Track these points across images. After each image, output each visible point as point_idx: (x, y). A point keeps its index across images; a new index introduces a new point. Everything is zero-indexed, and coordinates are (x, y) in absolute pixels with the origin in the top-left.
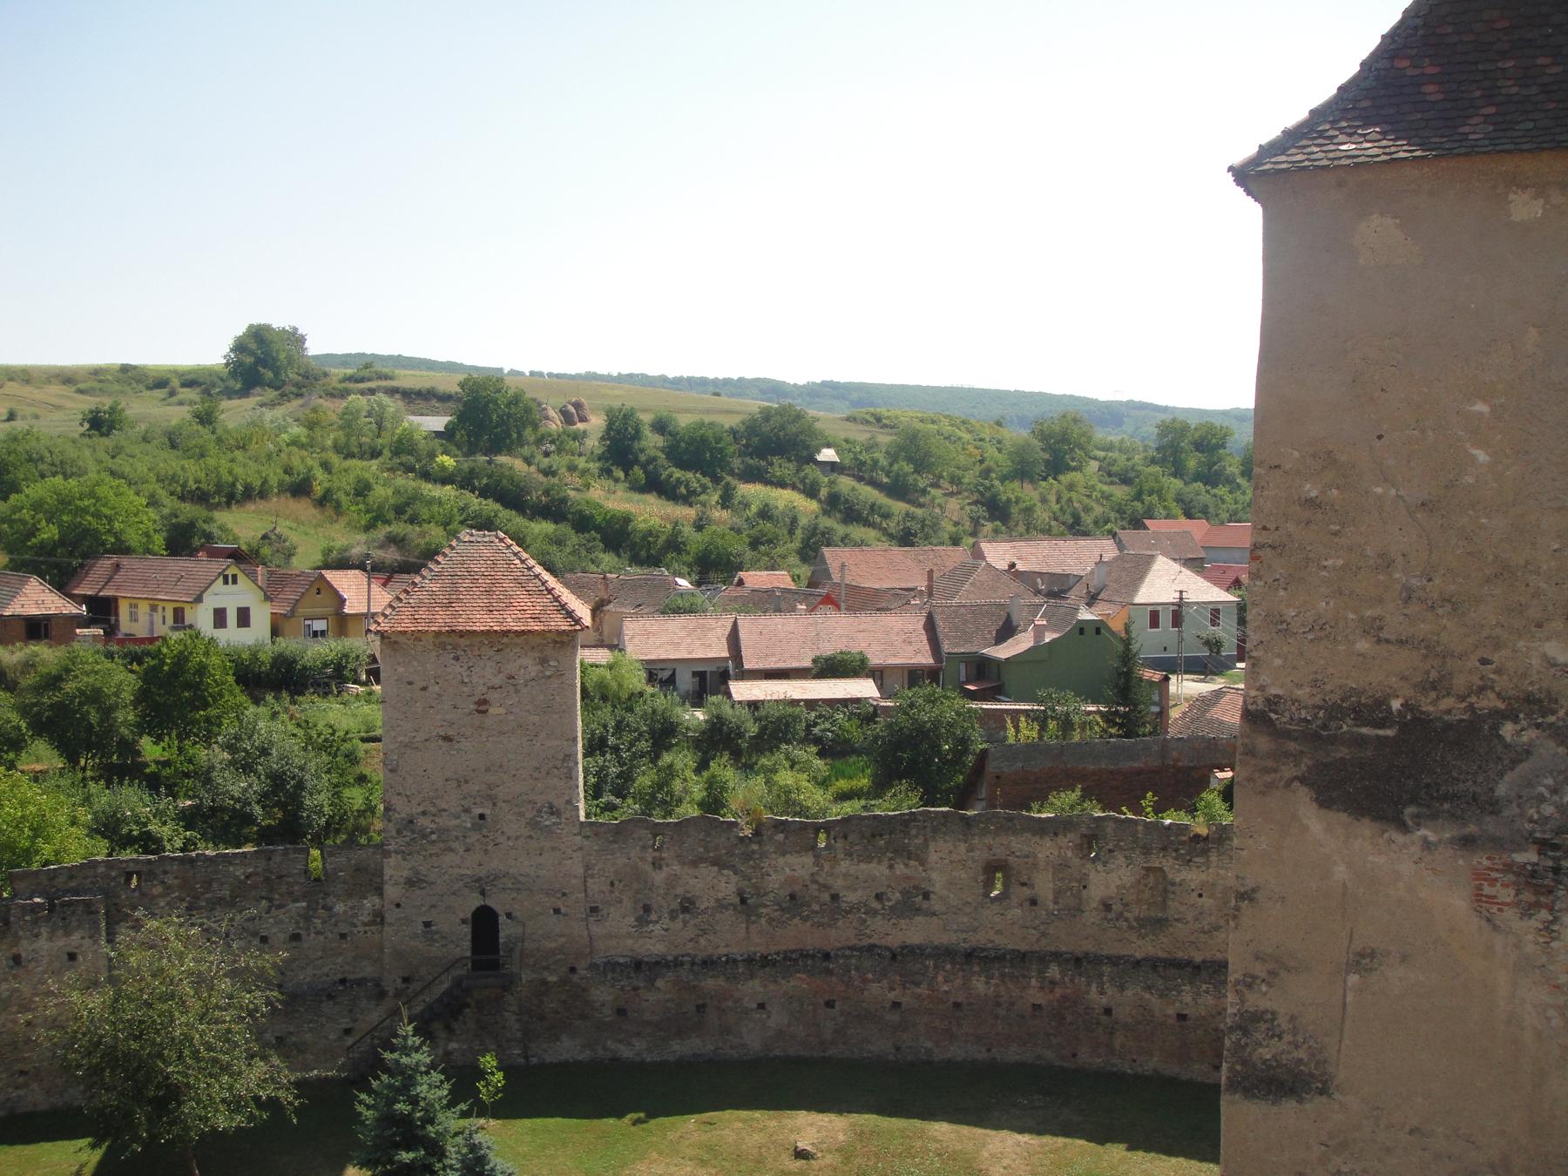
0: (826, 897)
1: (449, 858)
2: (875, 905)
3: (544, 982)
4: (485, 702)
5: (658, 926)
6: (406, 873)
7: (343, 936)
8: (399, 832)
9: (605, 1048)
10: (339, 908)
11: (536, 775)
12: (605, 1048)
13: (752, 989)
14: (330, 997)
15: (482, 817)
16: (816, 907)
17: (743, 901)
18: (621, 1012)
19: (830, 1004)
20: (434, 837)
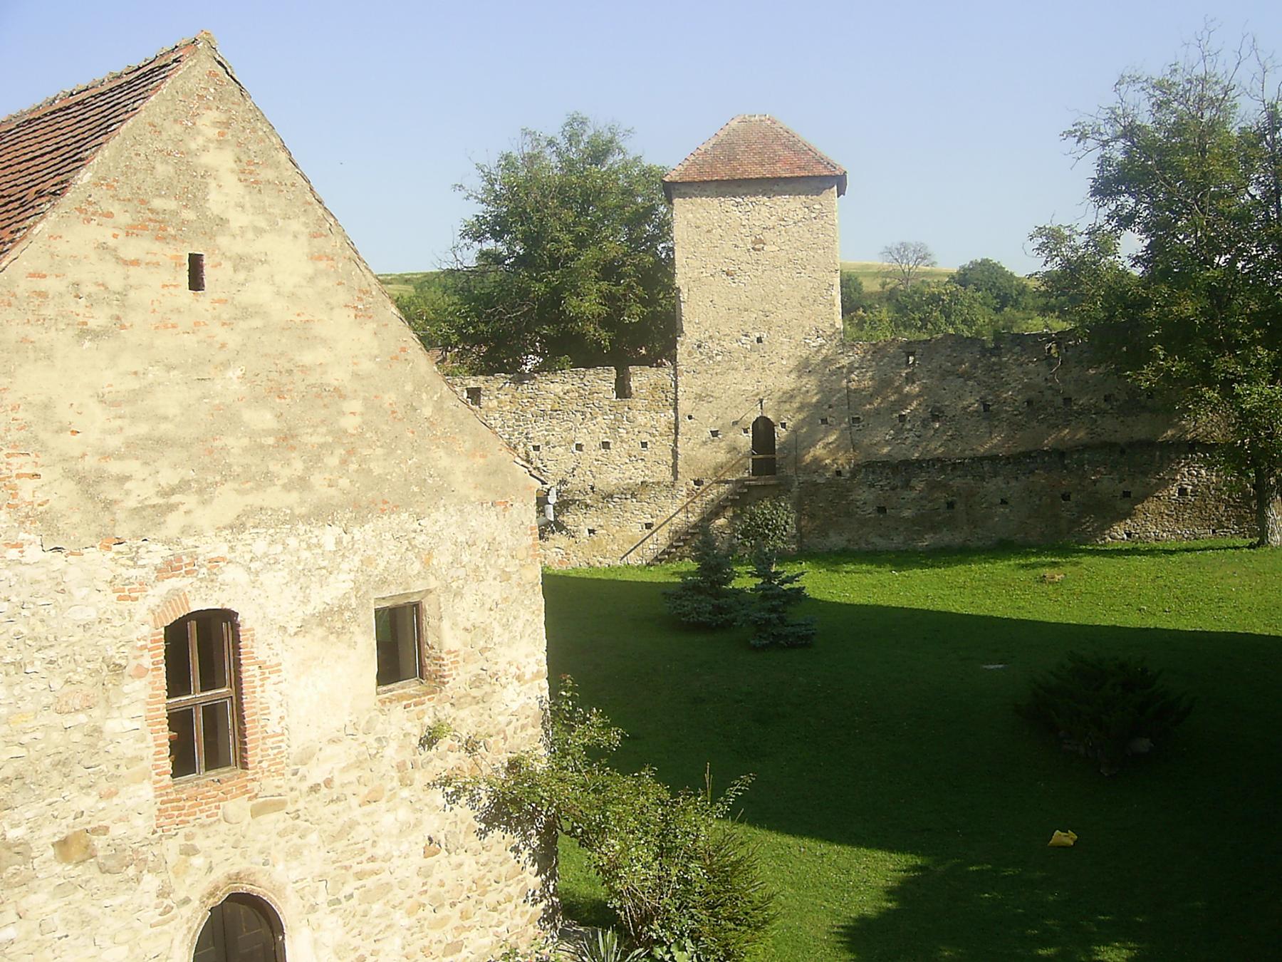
0: (1059, 401)
1: (732, 377)
2: (1103, 405)
3: (815, 484)
4: (761, 241)
5: (912, 434)
6: (696, 390)
7: (644, 445)
8: (690, 354)
9: (867, 543)
10: (641, 419)
11: (804, 303)
12: (867, 543)
13: (994, 486)
14: (633, 495)
15: (759, 340)
16: (1051, 410)
17: (986, 408)
18: (882, 510)
19: (1066, 497)
20: (719, 358)
